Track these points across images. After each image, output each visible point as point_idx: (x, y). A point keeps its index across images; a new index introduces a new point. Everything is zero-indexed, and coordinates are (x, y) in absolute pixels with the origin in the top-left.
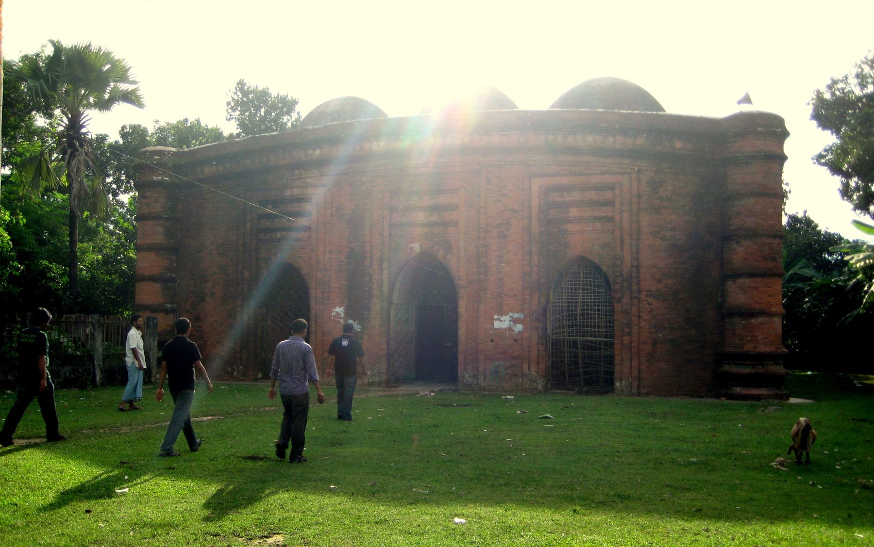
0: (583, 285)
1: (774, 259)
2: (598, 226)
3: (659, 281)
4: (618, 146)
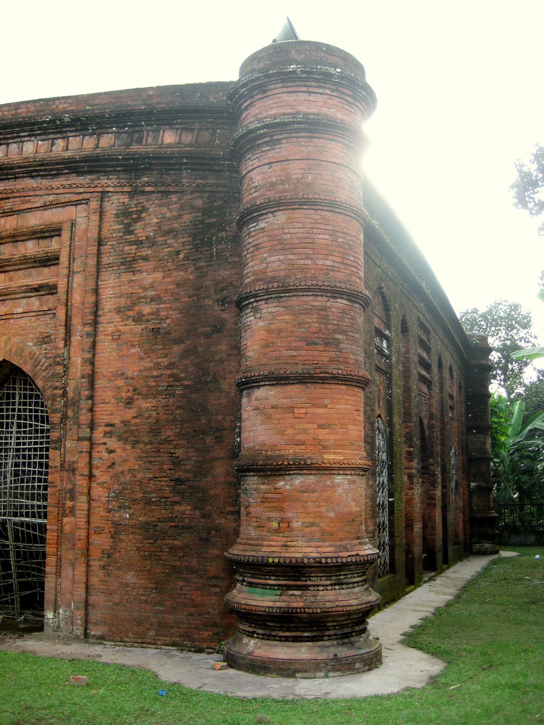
0: (19, 418)
1: (329, 343)
2: (35, 303)
3: (129, 402)
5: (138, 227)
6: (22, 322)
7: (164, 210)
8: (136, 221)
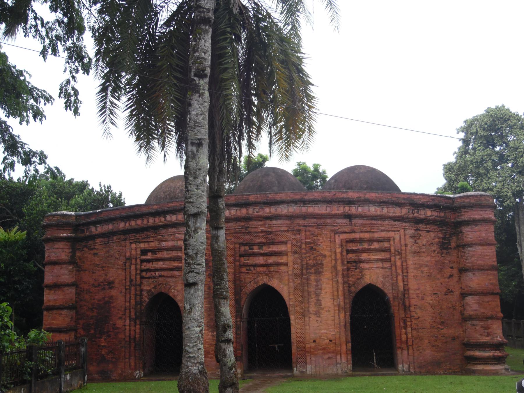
2: (380, 264)
4: (391, 214)
5: (419, 241)
6: (376, 270)
7: (428, 236)
8: (418, 239)
